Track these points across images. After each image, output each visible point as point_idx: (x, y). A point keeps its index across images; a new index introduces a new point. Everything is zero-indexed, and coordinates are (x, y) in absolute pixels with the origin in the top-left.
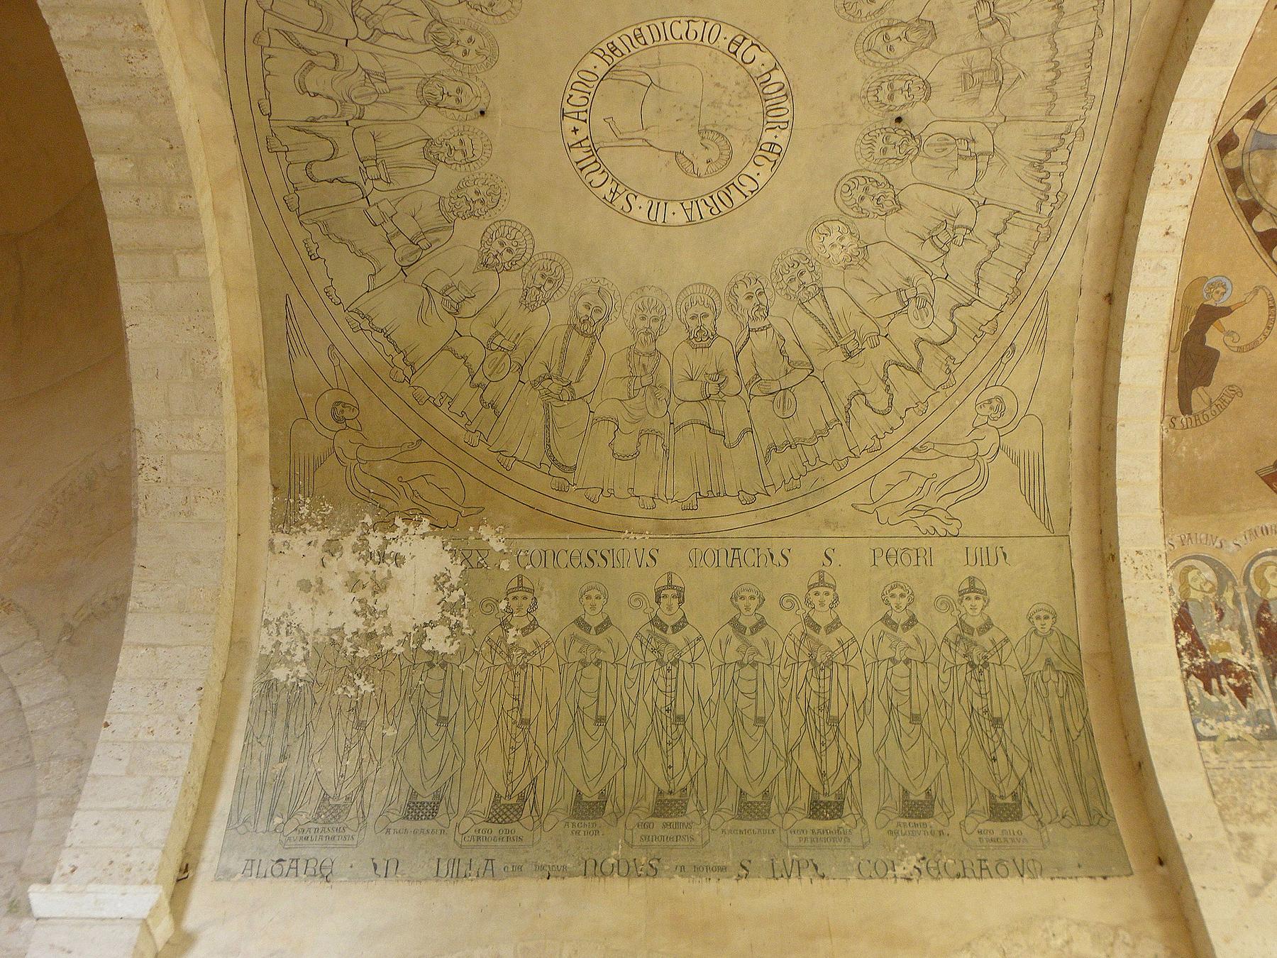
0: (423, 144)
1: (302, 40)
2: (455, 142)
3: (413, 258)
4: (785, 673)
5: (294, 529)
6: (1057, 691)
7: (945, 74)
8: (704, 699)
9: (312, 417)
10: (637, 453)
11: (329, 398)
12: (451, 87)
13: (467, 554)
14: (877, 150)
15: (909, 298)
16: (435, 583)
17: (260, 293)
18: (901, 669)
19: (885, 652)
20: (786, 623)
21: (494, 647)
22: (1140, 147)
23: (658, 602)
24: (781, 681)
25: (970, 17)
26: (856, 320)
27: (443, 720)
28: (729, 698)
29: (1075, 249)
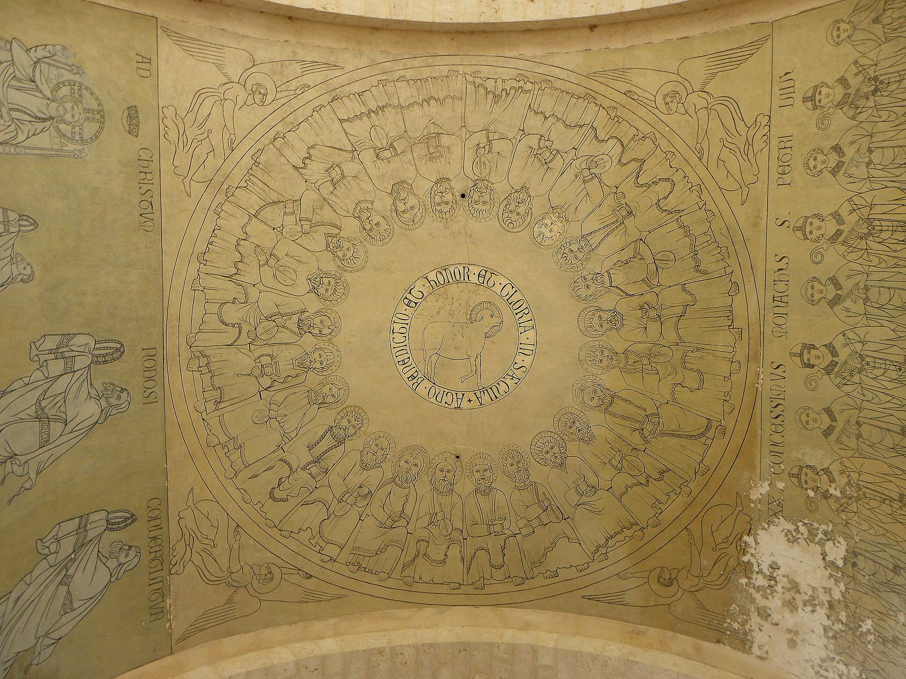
0: (479, 495)
1: (408, 559)
2: (478, 476)
3: (557, 511)
4: (875, 261)
5: (749, 637)
6: (901, 8)
7: (431, 171)
8: (892, 335)
9: (668, 601)
10: (698, 371)
11: (655, 586)
12: (439, 475)
13: (772, 513)
14: (484, 207)
15: (590, 173)
16: (793, 542)
17: (581, 614)
18: (876, 157)
19: (861, 172)
20: (834, 259)
21: (843, 509)
22: (485, 32)
23: (813, 366)
24: (882, 265)
25: (389, 162)
26: (605, 210)
27: (896, 569)
28: (894, 313)
29: (557, 61)
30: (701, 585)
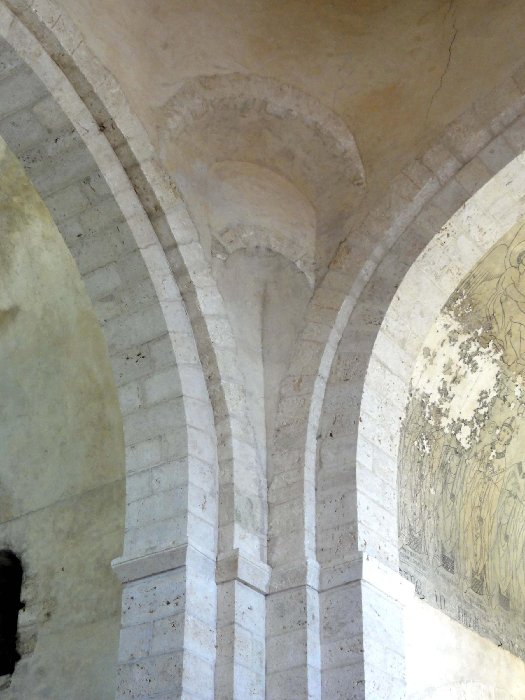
16: (480, 395)
27: (453, 496)
30: (500, 288)
